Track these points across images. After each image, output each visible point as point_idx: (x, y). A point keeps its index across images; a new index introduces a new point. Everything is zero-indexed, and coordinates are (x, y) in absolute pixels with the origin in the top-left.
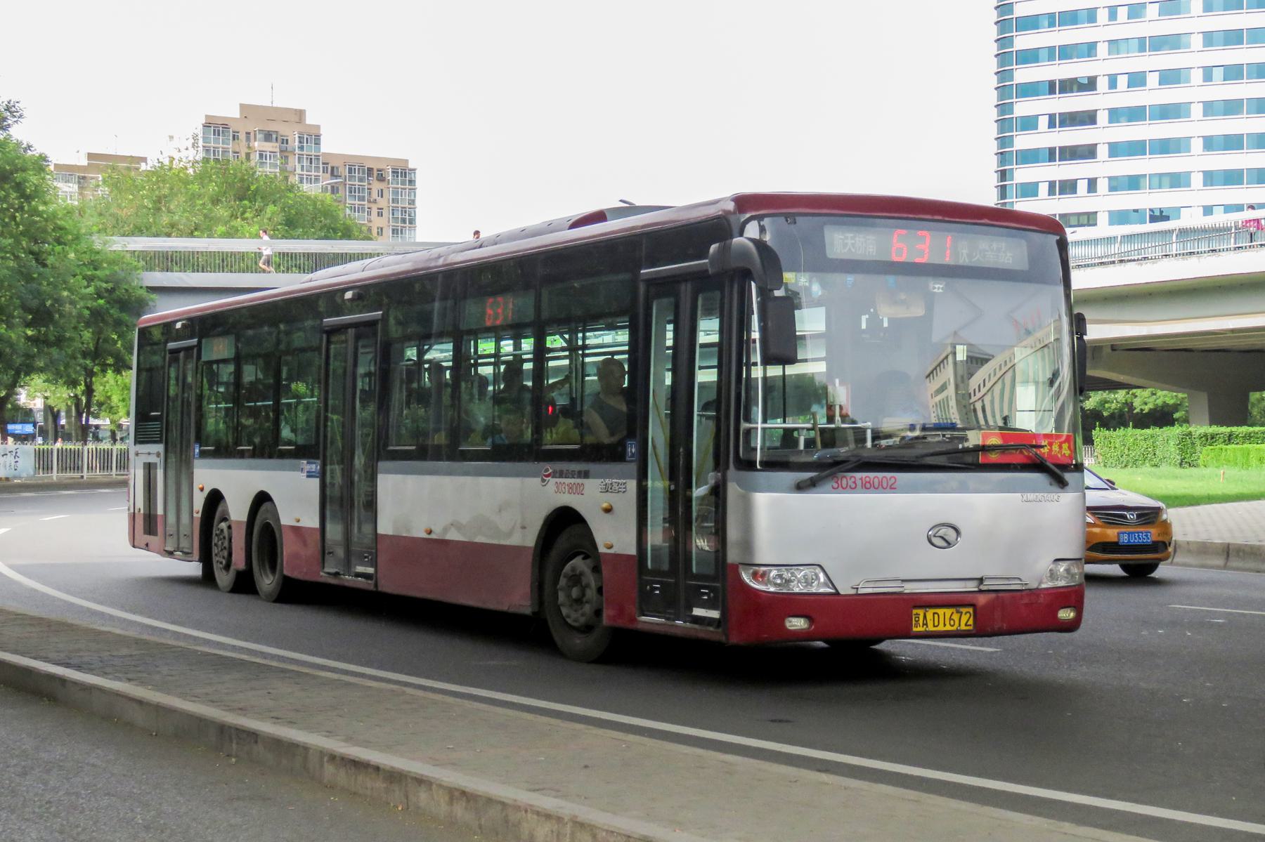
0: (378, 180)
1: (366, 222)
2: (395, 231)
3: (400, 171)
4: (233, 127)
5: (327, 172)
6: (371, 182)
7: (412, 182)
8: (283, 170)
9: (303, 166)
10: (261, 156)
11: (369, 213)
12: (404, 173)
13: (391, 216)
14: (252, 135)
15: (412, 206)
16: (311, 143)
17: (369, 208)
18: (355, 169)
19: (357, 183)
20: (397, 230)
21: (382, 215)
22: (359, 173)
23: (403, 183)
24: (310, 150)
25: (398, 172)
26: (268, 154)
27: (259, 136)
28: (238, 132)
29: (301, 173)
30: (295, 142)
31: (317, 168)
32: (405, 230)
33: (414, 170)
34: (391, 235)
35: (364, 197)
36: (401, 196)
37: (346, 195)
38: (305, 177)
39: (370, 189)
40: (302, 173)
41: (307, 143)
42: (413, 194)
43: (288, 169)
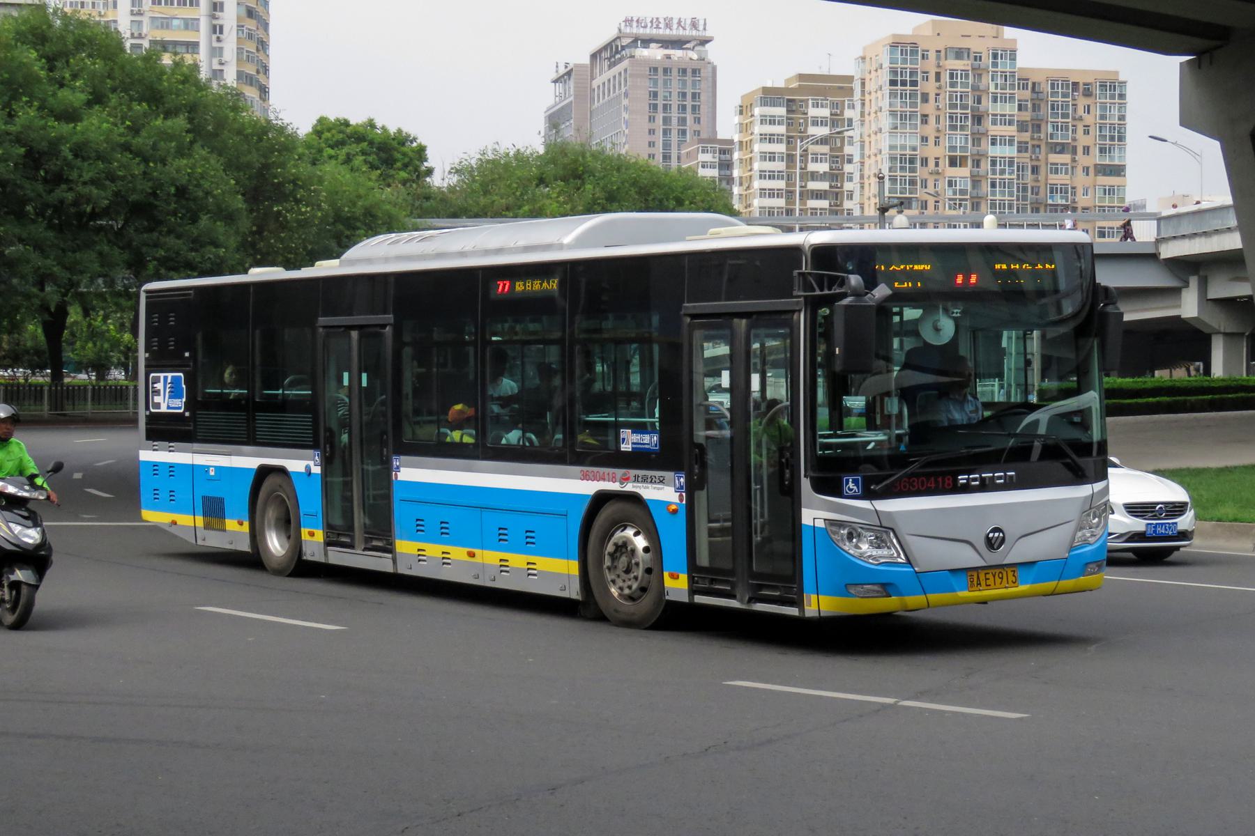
1: (1070, 141)
2: (1102, 150)
3: (1108, 84)
5: (1027, 89)
6: (1076, 97)
7: (1122, 96)
8: (975, 88)
9: (996, 88)
10: (952, 76)
11: (1074, 131)
13: (1098, 133)
14: (943, 54)
15: (1122, 122)
18: (1058, 84)
19: (1060, 99)
21: (1088, 133)
22: (1062, 88)
23: (1112, 97)
24: (1004, 66)
25: (1106, 86)
26: (959, 72)
28: (928, 51)
29: (994, 91)
32: (1114, 148)
33: (1125, 83)
34: (1098, 154)
39: (1075, 105)
41: (1002, 58)
43: (982, 87)
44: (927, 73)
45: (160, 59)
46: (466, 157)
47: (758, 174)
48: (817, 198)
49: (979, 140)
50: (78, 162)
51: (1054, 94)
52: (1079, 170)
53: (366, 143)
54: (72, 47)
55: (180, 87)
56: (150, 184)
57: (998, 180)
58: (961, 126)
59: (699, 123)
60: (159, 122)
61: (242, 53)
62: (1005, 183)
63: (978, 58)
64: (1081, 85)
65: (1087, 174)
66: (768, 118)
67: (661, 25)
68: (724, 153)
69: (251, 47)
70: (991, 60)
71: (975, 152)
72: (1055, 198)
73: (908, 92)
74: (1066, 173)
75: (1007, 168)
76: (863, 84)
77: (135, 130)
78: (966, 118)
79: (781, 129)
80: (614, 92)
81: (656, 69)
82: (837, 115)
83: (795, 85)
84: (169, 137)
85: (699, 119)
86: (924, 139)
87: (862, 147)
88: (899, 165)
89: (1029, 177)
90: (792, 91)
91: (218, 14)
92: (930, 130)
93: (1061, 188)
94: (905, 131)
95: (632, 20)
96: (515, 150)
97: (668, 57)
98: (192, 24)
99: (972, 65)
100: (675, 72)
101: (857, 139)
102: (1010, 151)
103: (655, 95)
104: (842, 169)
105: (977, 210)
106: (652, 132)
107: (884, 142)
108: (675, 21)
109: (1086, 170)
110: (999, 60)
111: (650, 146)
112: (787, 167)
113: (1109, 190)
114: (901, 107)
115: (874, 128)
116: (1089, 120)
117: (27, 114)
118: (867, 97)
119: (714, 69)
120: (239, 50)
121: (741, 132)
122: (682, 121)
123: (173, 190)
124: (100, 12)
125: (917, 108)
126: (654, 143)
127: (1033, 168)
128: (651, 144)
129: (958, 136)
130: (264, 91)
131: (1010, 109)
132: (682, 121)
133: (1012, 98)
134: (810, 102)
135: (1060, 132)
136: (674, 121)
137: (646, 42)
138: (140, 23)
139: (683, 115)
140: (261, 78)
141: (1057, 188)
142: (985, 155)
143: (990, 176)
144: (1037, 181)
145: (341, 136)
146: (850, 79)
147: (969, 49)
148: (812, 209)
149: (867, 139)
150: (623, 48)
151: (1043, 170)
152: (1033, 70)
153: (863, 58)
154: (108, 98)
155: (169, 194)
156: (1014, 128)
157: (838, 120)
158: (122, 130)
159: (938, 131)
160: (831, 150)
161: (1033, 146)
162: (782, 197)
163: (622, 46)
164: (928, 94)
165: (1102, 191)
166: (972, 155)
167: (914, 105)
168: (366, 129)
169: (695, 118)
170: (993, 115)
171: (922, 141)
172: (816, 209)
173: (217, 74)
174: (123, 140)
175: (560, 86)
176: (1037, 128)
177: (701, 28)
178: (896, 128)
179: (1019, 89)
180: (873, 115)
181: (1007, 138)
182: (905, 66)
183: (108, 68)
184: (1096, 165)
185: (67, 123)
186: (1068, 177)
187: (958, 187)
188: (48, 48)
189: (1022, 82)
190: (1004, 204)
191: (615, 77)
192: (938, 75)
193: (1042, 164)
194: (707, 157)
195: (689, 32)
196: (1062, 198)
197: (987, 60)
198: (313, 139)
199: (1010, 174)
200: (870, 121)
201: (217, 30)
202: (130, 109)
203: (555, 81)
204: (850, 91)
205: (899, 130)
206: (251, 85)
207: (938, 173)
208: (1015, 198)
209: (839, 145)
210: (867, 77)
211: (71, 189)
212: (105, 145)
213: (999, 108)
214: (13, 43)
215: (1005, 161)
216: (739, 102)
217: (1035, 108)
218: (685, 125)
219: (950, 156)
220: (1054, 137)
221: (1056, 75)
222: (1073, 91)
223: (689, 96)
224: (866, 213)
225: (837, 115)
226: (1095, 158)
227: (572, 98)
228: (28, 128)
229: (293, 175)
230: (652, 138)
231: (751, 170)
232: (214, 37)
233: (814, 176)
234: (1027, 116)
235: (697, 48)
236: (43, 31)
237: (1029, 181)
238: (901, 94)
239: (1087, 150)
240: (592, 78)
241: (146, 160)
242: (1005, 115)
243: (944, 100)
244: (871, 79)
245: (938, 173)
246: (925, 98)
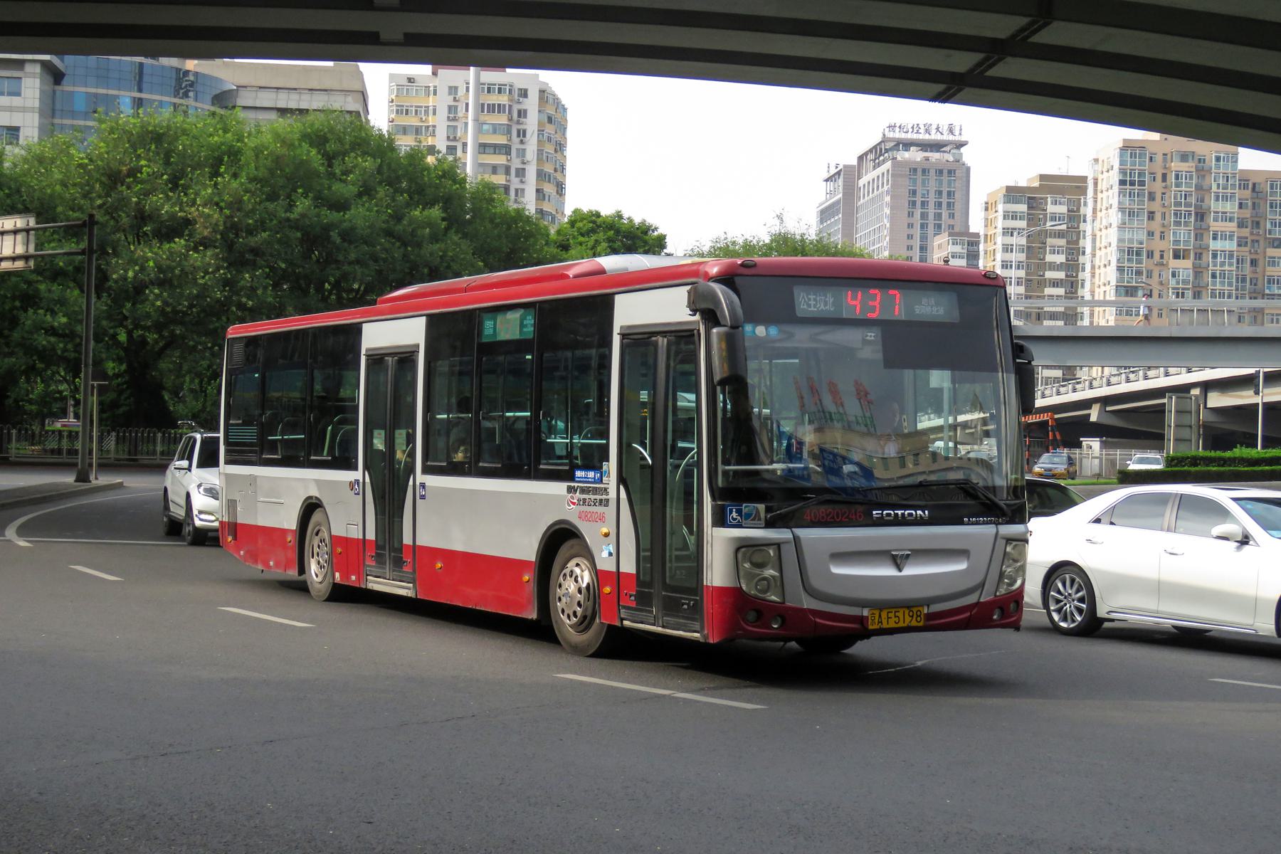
4: (1151, 149)
8: (1199, 188)
9: (1218, 188)
10: (1177, 177)
14: (1169, 156)
16: (1228, 161)
28: (1155, 154)
41: (1224, 161)
43: (1205, 187)
45: (426, 158)
46: (698, 244)
47: (1000, 263)
48: (1054, 286)
49: (1202, 234)
50: (346, 244)
53: (612, 232)
54: (347, 147)
55: (438, 182)
56: (408, 265)
58: (1185, 222)
59: (953, 218)
60: (417, 213)
61: (542, 154)
66: (1011, 214)
67: (920, 131)
68: (972, 245)
69: (549, 149)
71: (1198, 246)
73: (1136, 191)
75: (1227, 260)
76: (1096, 184)
77: (398, 218)
78: (1190, 214)
79: (1022, 224)
80: (878, 189)
81: (915, 170)
82: (1074, 212)
83: (1036, 184)
84: (430, 224)
85: (953, 214)
86: (1151, 234)
87: (1094, 241)
88: (1126, 256)
91: (522, 120)
92: (1156, 225)
95: (895, 126)
96: (743, 238)
97: (927, 159)
98: (500, 129)
99: (1196, 167)
100: (932, 172)
101: (1089, 233)
102: (1231, 245)
103: (914, 192)
104: (1078, 260)
105: (1199, 298)
106: (910, 226)
107: (1112, 236)
108: (934, 127)
111: (908, 238)
112: (1027, 258)
115: (1104, 223)
117: (303, 205)
118: (1100, 196)
119: (968, 169)
120: (540, 152)
121: (986, 226)
122: (938, 216)
123: (426, 271)
124: (421, 118)
126: (912, 236)
128: (910, 237)
130: (560, 188)
131: (1230, 207)
132: (938, 216)
134: (1049, 199)
136: (931, 216)
137: (907, 145)
138: (455, 127)
139: (939, 211)
140: (558, 176)
141: (1274, 279)
142: (1207, 248)
143: (1210, 268)
144: (1255, 272)
145: (591, 225)
146: (1084, 179)
148: (1049, 296)
149: (1098, 234)
150: (887, 151)
151: (1261, 263)
153: (1096, 160)
154: (376, 191)
155: (423, 274)
156: (1235, 224)
158: (384, 217)
159: (1163, 226)
160: (1068, 242)
161: (1253, 241)
162: (1022, 285)
163: (885, 149)
166: (1194, 248)
168: (614, 222)
169: (950, 214)
170: (1214, 212)
171: (1149, 235)
172: (1053, 296)
173: (521, 173)
174: (384, 226)
175: (831, 185)
177: (957, 133)
179: (1240, 188)
181: (1228, 233)
182: (1132, 167)
183: (377, 165)
185: (339, 212)
187: (1181, 278)
188: (331, 147)
189: (1243, 182)
190: (1224, 293)
191: (878, 177)
192: (1164, 177)
193: (1260, 257)
194: (958, 249)
195: (946, 137)
198: (566, 228)
200: (1101, 218)
201: (522, 133)
202: (393, 200)
203: (827, 180)
204: (1083, 191)
206: (549, 181)
207: (1162, 264)
208: (1234, 288)
209: (1075, 238)
210: (1100, 177)
211: (338, 269)
212: (369, 230)
214: (297, 143)
215: (1225, 255)
216: (986, 200)
218: (941, 220)
220: (1273, 232)
223: (945, 194)
224: (1096, 298)
227: (841, 195)
228: (303, 216)
229: (534, 258)
230: (911, 231)
231: (994, 260)
232: (519, 139)
233: (1053, 267)
235: (952, 151)
236: (325, 133)
238: (1130, 193)
240: (859, 179)
241: (405, 244)
242: (1226, 213)
245: (1162, 264)
246: (1152, 197)
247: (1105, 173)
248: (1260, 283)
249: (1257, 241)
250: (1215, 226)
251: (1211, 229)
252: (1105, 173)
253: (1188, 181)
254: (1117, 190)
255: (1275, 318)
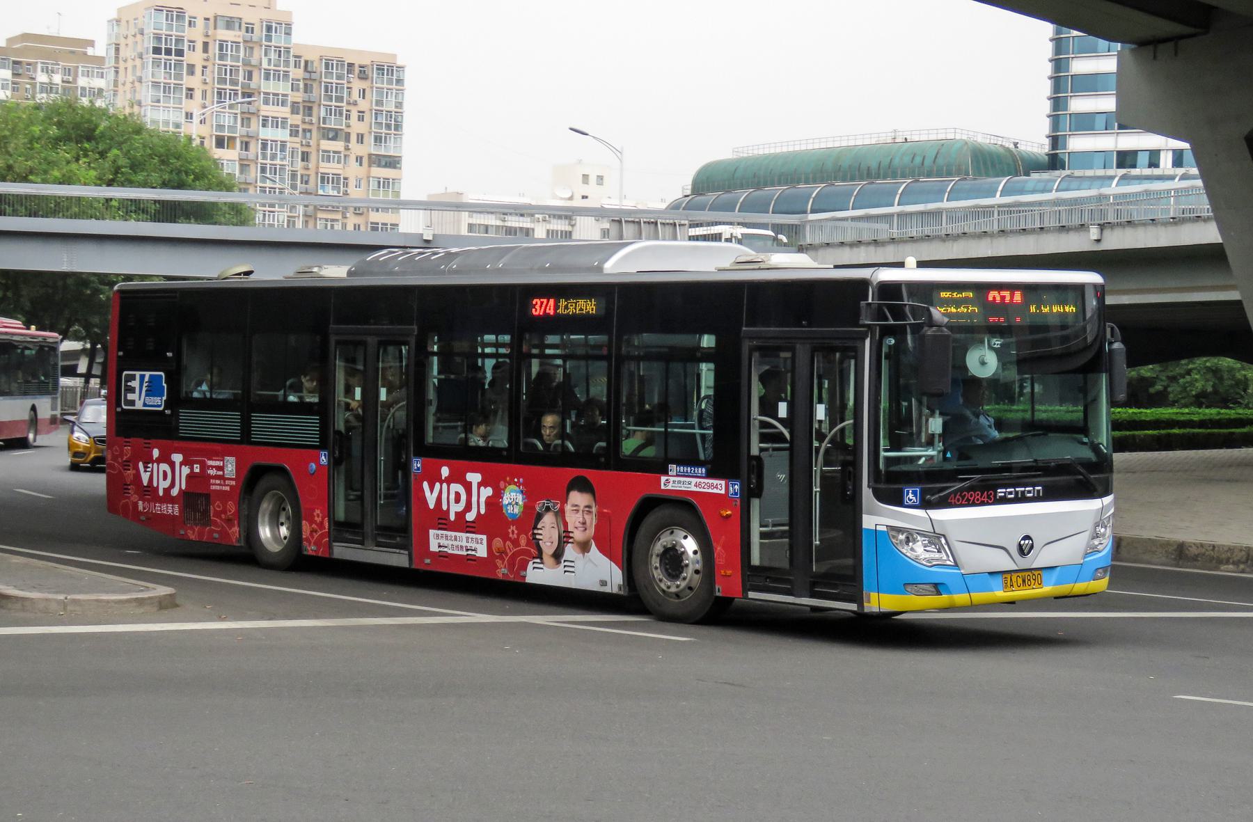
0: (360, 78)
1: (343, 127)
2: (378, 139)
3: (386, 68)
5: (299, 68)
6: (352, 80)
7: (399, 81)
8: (247, 63)
9: (270, 60)
10: (221, 48)
11: (348, 117)
12: (389, 71)
13: (374, 121)
16: (280, 33)
17: (347, 111)
18: (332, 64)
19: (334, 81)
20: (381, 137)
21: (363, 120)
22: (337, 69)
23: (390, 82)
25: (383, 69)
26: (229, 44)
27: (220, 23)
28: (195, 18)
30: (262, 31)
31: (287, 63)
32: (390, 138)
34: (373, 143)
35: (343, 97)
36: (387, 98)
37: (321, 95)
38: (272, 72)
40: (269, 68)
41: (276, 32)
42: (400, 95)
43: (254, 62)
44: (193, 42)
51: (329, 74)
52: (353, 158)
57: (268, 166)
62: (275, 169)
63: (250, 30)
64: (357, 66)
65: (361, 165)
70: (264, 33)
72: (326, 188)
73: (173, 62)
74: (339, 162)
75: (279, 153)
76: (117, 50)
82: (69, 82)
86: (189, 116)
89: (299, 165)
90: (19, 52)
93: (333, 178)
94: (167, 105)
102: (282, 135)
109: (359, 160)
110: (273, 34)
113: (384, 182)
114: (165, 78)
116: (363, 105)
118: (122, 65)
125: (182, 80)
127: (303, 153)
129: (227, 115)
131: (282, 88)
133: (286, 75)
134: (39, 66)
135: (333, 117)
141: (328, 178)
143: (260, 160)
144: (307, 169)
147: (241, 19)
151: (313, 158)
152: (306, 46)
153: (118, 21)
156: (287, 109)
157: (71, 88)
161: (304, 130)
164: (193, 66)
165: (376, 183)
167: (179, 76)
170: (265, 93)
171: (187, 118)
176: (309, 110)
178: (158, 101)
180: (128, 86)
181: (280, 119)
184: (370, 155)
186: (340, 166)
192: (206, 45)
193: (313, 150)
196: (333, 188)
197: (259, 33)
199: (282, 159)
200: (125, 92)
205: (161, 104)
210: (122, 42)
213: (271, 87)
217: (307, 89)
219: (216, 136)
220: (327, 121)
221: (330, 55)
222: (348, 73)
225: (69, 82)
226: (370, 147)
234: (299, 97)
237: (298, 169)
238: (165, 63)
239: (361, 138)
242: (278, 95)
243: (212, 74)
244: (127, 45)
246: (191, 70)
247: (131, 40)
248: (312, 179)
249: (310, 131)
250: (269, 110)
251: (262, 113)
252: (131, 40)
253: (234, 53)
254: (151, 60)
255: (329, 224)
